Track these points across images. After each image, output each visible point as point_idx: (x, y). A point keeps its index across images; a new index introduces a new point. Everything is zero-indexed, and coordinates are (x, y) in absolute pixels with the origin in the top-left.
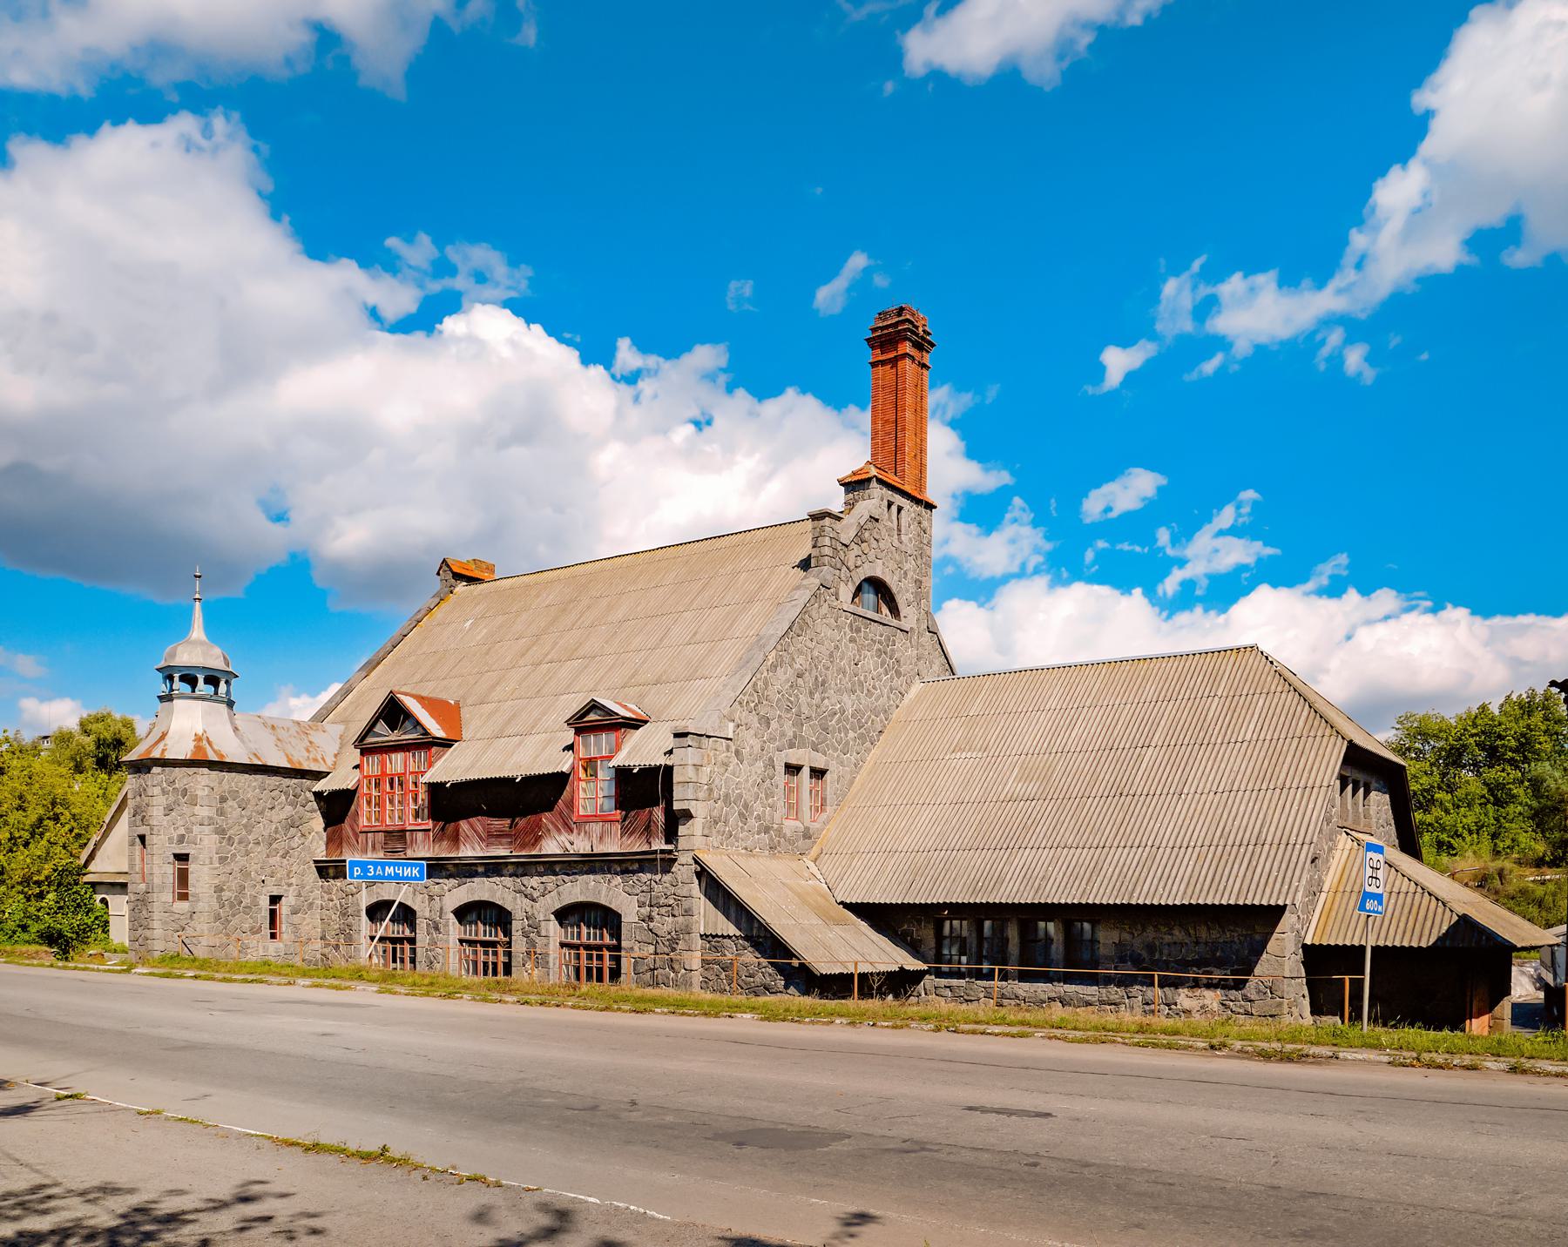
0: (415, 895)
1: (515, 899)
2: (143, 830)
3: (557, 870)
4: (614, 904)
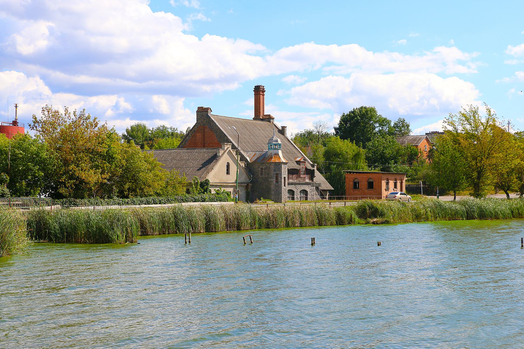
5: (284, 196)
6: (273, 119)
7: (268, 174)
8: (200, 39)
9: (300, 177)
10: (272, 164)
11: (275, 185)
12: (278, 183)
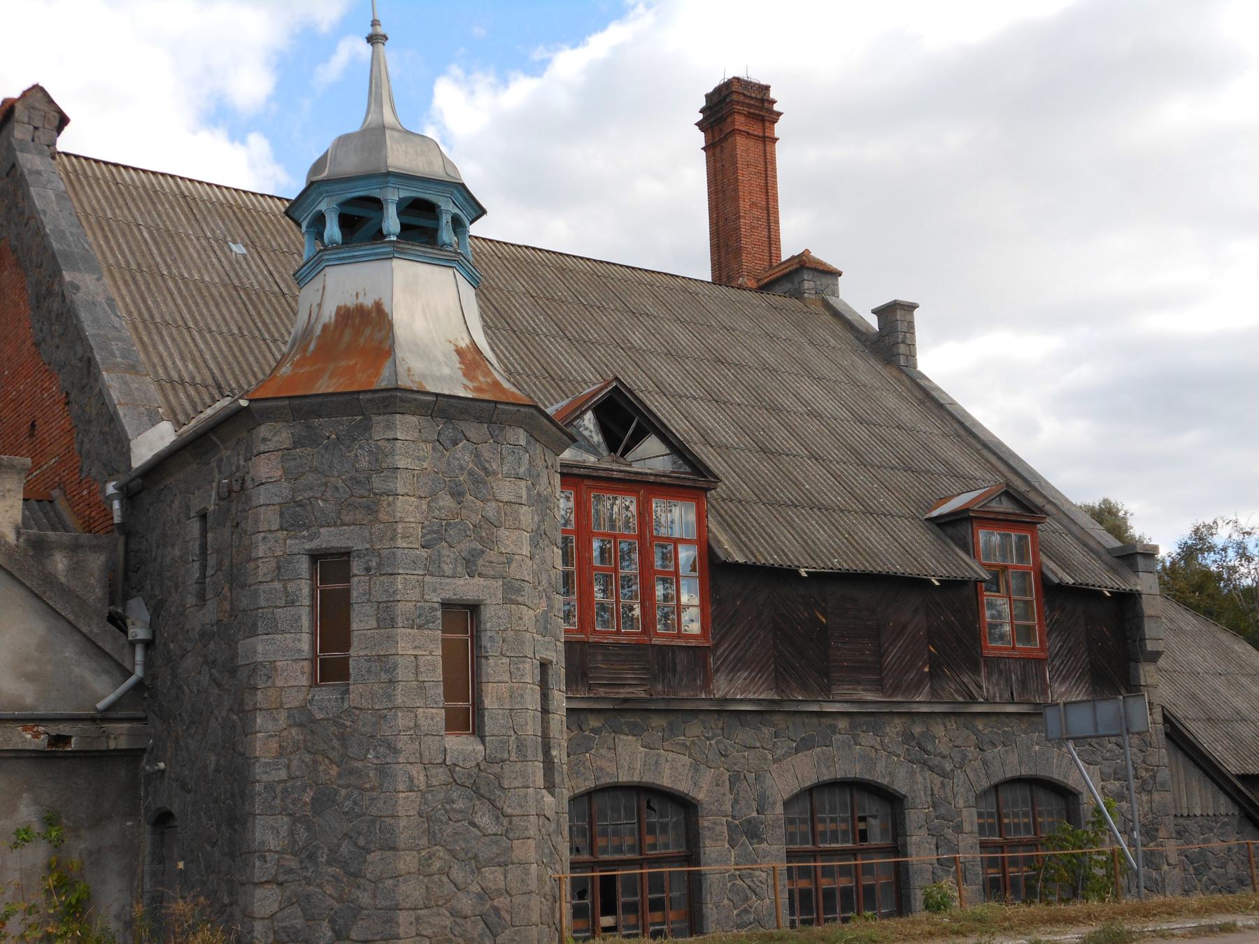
0: (697, 771)
1: (913, 773)
2: (466, 588)
4: (1071, 778)
5: (458, 874)
6: (836, 274)
7: (237, 578)
10: (264, 430)
11: (304, 719)
12: (347, 692)
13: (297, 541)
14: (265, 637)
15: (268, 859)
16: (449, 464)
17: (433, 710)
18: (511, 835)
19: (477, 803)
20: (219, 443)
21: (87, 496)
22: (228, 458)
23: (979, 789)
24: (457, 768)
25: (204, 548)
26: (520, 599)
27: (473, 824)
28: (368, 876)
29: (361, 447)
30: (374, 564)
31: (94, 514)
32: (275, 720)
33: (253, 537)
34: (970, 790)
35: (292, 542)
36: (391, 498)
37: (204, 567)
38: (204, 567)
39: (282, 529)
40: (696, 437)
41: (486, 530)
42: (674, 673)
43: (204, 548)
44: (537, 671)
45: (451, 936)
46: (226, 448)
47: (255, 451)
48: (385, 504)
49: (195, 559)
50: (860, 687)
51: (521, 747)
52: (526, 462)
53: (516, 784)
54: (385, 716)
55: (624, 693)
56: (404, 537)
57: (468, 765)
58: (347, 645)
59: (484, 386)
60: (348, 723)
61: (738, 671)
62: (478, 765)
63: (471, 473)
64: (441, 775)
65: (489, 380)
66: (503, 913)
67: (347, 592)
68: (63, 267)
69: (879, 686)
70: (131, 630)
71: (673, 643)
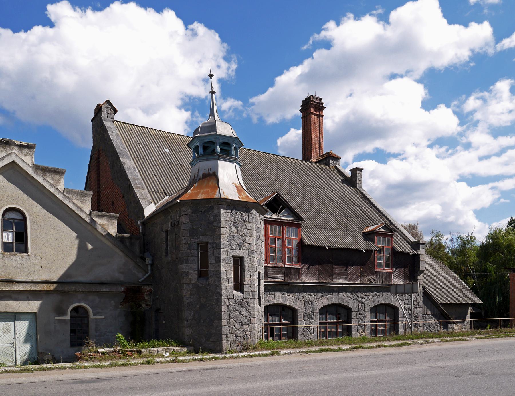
1: (354, 302)
3: (373, 290)
8: (301, 118)
9: (373, 272)
12: (207, 280)
13: (194, 239)
14: (186, 265)
15: (188, 321)
16: (234, 218)
17: (231, 285)
18: (250, 317)
19: (242, 308)
20: (171, 211)
21: (131, 224)
22: (174, 216)
23: (371, 307)
24: (237, 300)
25: (167, 240)
26: (253, 256)
27: (241, 314)
28: (214, 326)
29: (211, 214)
30: (214, 246)
31: (133, 229)
32: (189, 286)
33: (182, 238)
34: (369, 307)
35: (193, 239)
36: (219, 228)
37: (167, 245)
38: (167, 245)
39: (189, 236)
40: (298, 208)
41: (244, 238)
42: (291, 275)
43: (167, 240)
44: (257, 275)
45: (235, 341)
46: (173, 213)
47: (181, 214)
48: (217, 230)
49: (165, 243)
50: (341, 279)
51: (253, 294)
52: (255, 218)
53: (252, 304)
54: (218, 286)
55: (277, 280)
56: (223, 239)
57: (239, 299)
58: (207, 267)
59: (244, 197)
60: (208, 288)
61: (308, 274)
62: (242, 299)
63: (240, 222)
64: (232, 301)
65: (245, 195)
66: (248, 336)
67: (207, 253)
68: (120, 157)
69: (346, 279)
70: (147, 261)
71: (291, 267)
